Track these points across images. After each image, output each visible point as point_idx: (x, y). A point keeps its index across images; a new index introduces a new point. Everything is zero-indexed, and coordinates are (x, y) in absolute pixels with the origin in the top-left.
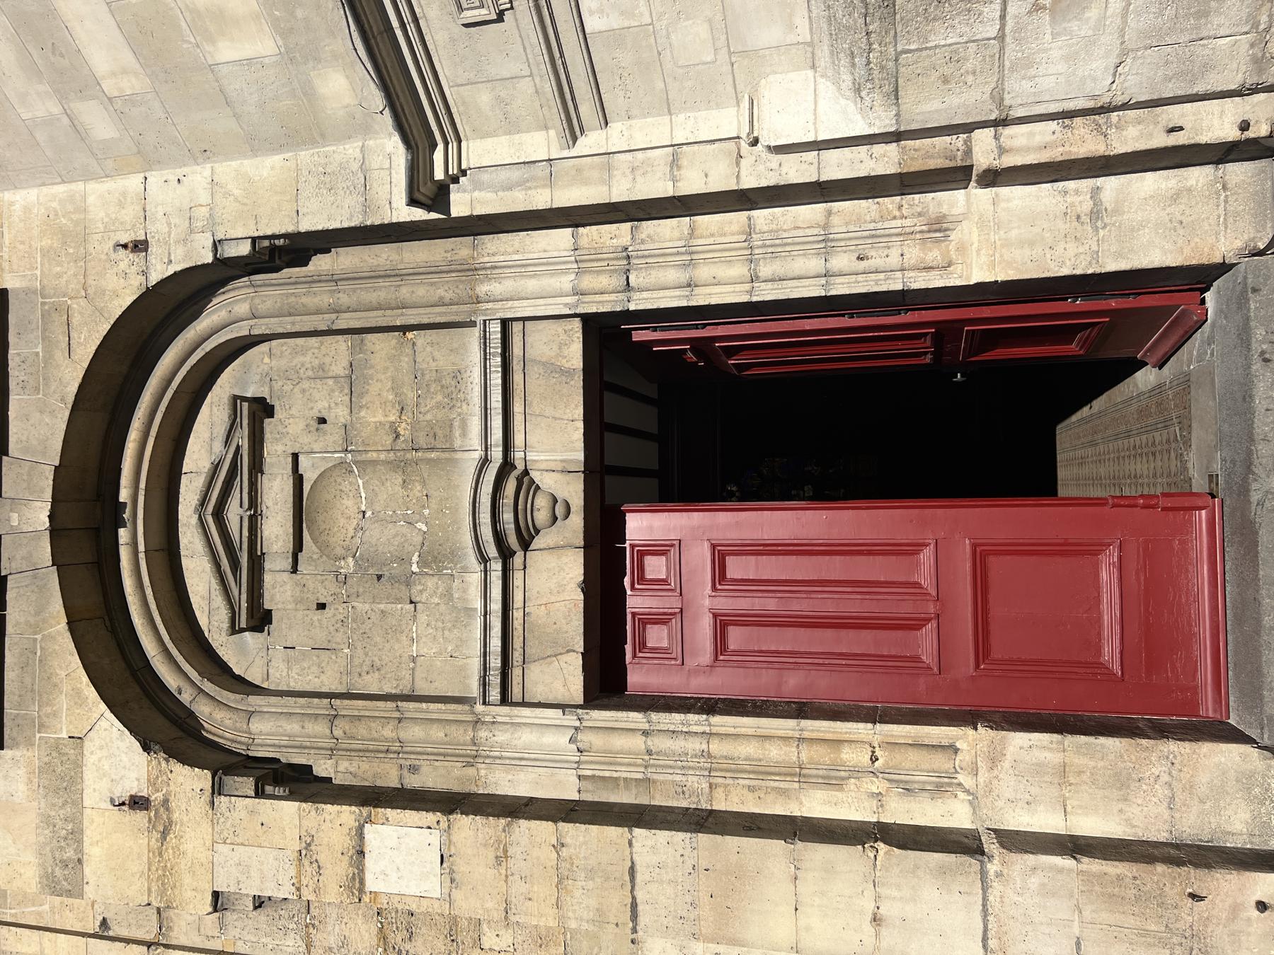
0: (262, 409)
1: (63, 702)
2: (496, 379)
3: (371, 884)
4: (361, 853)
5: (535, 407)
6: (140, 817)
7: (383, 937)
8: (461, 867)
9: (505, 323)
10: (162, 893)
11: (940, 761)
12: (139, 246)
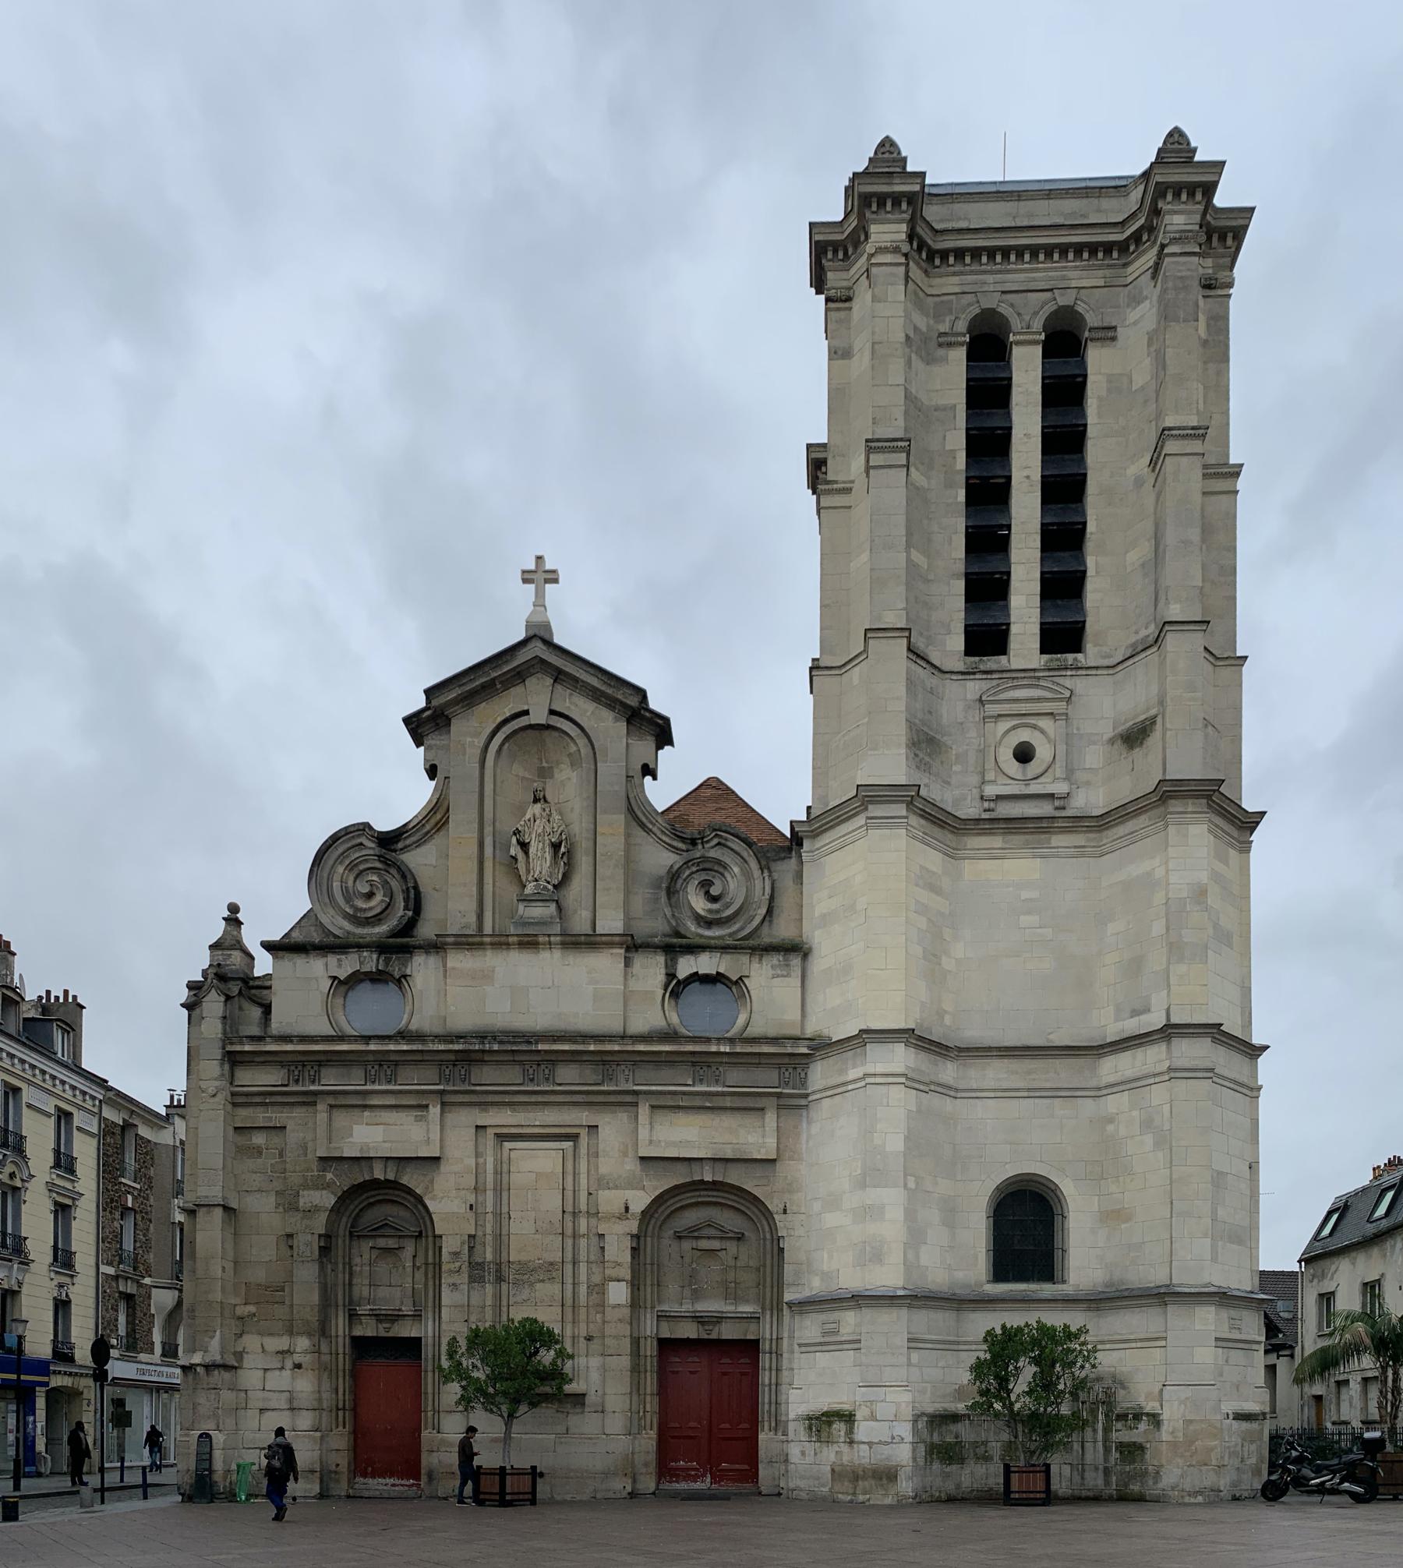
0: (740, 1238)
1: (655, 1183)
2: (745, 1315)
3: (610, 1283)
4: (618, 1281)
5: (737, 1325)
6: (623, 1210)
7: (596, 1285)
8: (617, 1310)
9: (759, 1318)
10: (603, 1217)
11: (648, 1427)
12: (785, 1211)
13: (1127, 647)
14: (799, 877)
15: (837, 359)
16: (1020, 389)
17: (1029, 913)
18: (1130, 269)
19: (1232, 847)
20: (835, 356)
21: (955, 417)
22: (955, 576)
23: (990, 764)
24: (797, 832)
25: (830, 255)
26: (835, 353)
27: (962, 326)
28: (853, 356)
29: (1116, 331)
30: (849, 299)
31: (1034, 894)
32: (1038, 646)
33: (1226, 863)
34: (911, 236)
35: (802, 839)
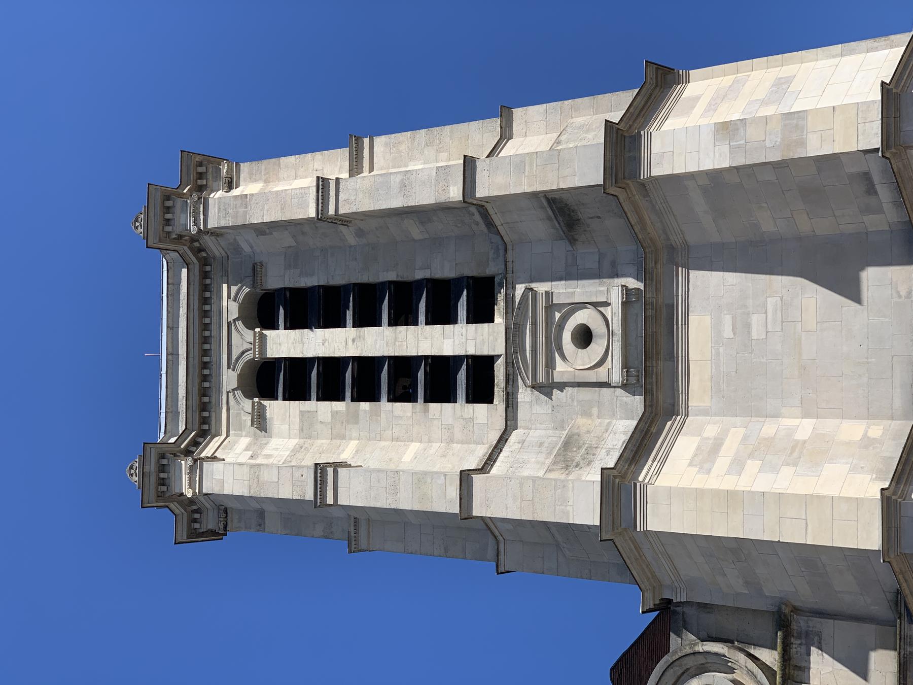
13: (490, 232)
14: (705, 607)
15: (265, 523)
16: (292, 350)
17: (748, 326)
18: (217, 254)
19: (682, 93)
20: (263, 526)
21: (308, 412)
22: (426, 411)
23: (592, 377)
24: (655, 605)
25: (197, 526)
26: (260, 525)
27: (247, 404)
28: (262, 509)
29: (256, 264)
30: (226, 511)
31: (727, 320)
32: (486, 325)
33: (698, 98)
34: (188, 453)
35: (663, 599)
